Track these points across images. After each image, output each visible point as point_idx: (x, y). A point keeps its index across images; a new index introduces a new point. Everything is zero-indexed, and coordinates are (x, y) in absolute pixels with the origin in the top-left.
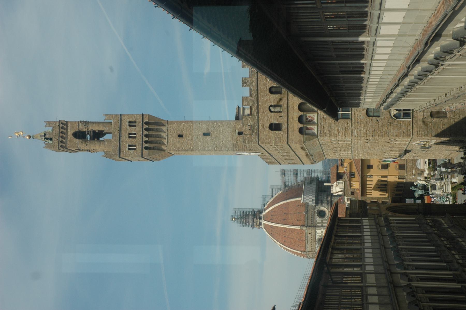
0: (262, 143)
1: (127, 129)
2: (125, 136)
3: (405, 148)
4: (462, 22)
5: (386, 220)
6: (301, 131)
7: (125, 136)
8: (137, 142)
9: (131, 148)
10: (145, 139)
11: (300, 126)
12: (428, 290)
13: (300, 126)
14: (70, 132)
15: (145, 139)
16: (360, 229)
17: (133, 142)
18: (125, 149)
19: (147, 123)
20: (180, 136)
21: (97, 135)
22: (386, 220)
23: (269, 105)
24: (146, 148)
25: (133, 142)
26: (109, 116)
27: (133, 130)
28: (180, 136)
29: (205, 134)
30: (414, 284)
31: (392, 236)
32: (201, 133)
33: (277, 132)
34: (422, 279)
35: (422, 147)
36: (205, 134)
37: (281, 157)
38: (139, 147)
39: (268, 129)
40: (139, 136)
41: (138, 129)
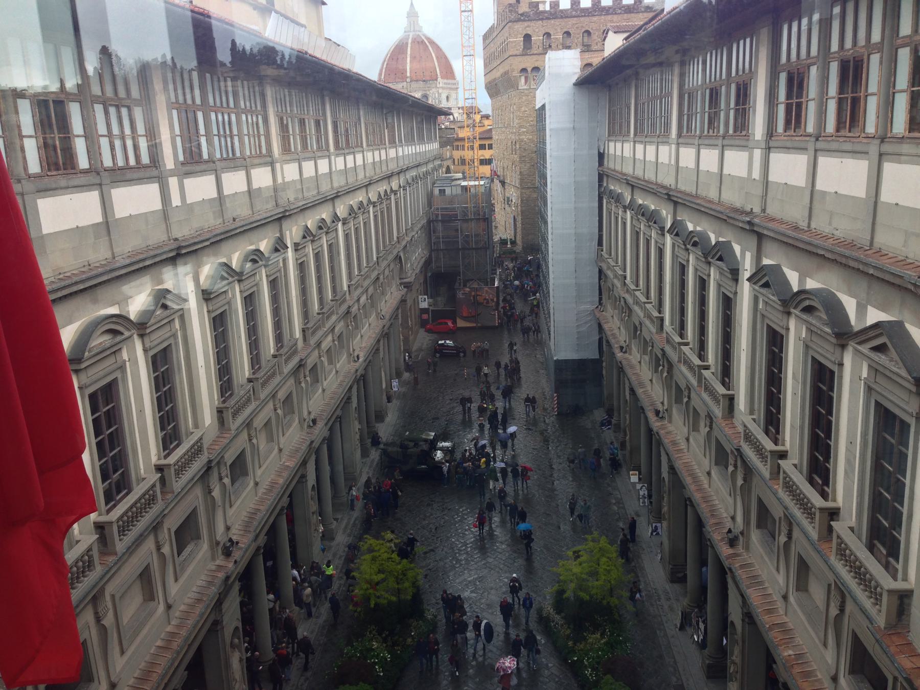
0: (510, 27)
3: (508, 181)
4: (695, 227)
5: (440, 166)
6: (524, 70)
11: (529, 70)
12: (389, 209)
13: (529, 70)
16: (430, 140)
22: (440, 166)
23: (552, 33)
30: (393, 197)
31: (427, 173)
33: (522, 43)
34: (396, 203)
35: (508, 198)
37: (492, 50)
39: (525, 33)
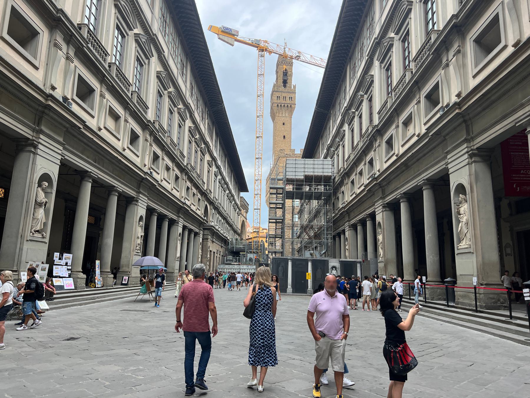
1: (288, 96)
2: (284, 95)
7: (284, 95)
8: (281, 101)
9: (278, 97)
10: (283, 105)
14: (287, 68)
15: (283, 105)
17: (282, 99)
18: (278, 94)
19: (291, 106)
20: (284, 124)
21: (285, 82)
24: (278, 105)
25: (282, 99)
26: (295, 87)
27: (288, 99)
28: (284, 124)
29: (284, 137)
32: (285, 134)
36: (284, 137)
38: (279, 101)
40: (284, 102)
41: (288, 101)
